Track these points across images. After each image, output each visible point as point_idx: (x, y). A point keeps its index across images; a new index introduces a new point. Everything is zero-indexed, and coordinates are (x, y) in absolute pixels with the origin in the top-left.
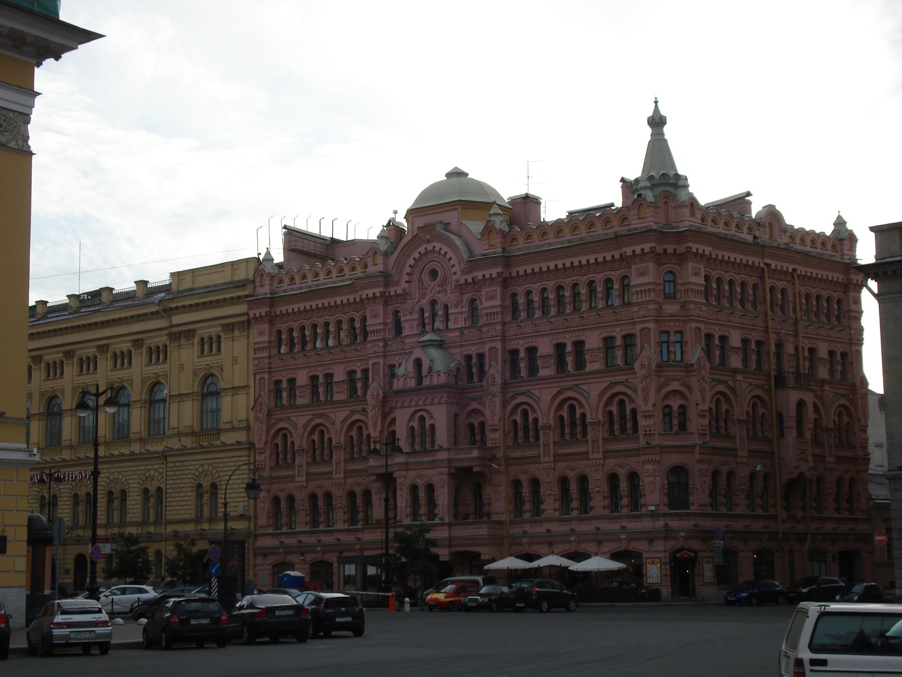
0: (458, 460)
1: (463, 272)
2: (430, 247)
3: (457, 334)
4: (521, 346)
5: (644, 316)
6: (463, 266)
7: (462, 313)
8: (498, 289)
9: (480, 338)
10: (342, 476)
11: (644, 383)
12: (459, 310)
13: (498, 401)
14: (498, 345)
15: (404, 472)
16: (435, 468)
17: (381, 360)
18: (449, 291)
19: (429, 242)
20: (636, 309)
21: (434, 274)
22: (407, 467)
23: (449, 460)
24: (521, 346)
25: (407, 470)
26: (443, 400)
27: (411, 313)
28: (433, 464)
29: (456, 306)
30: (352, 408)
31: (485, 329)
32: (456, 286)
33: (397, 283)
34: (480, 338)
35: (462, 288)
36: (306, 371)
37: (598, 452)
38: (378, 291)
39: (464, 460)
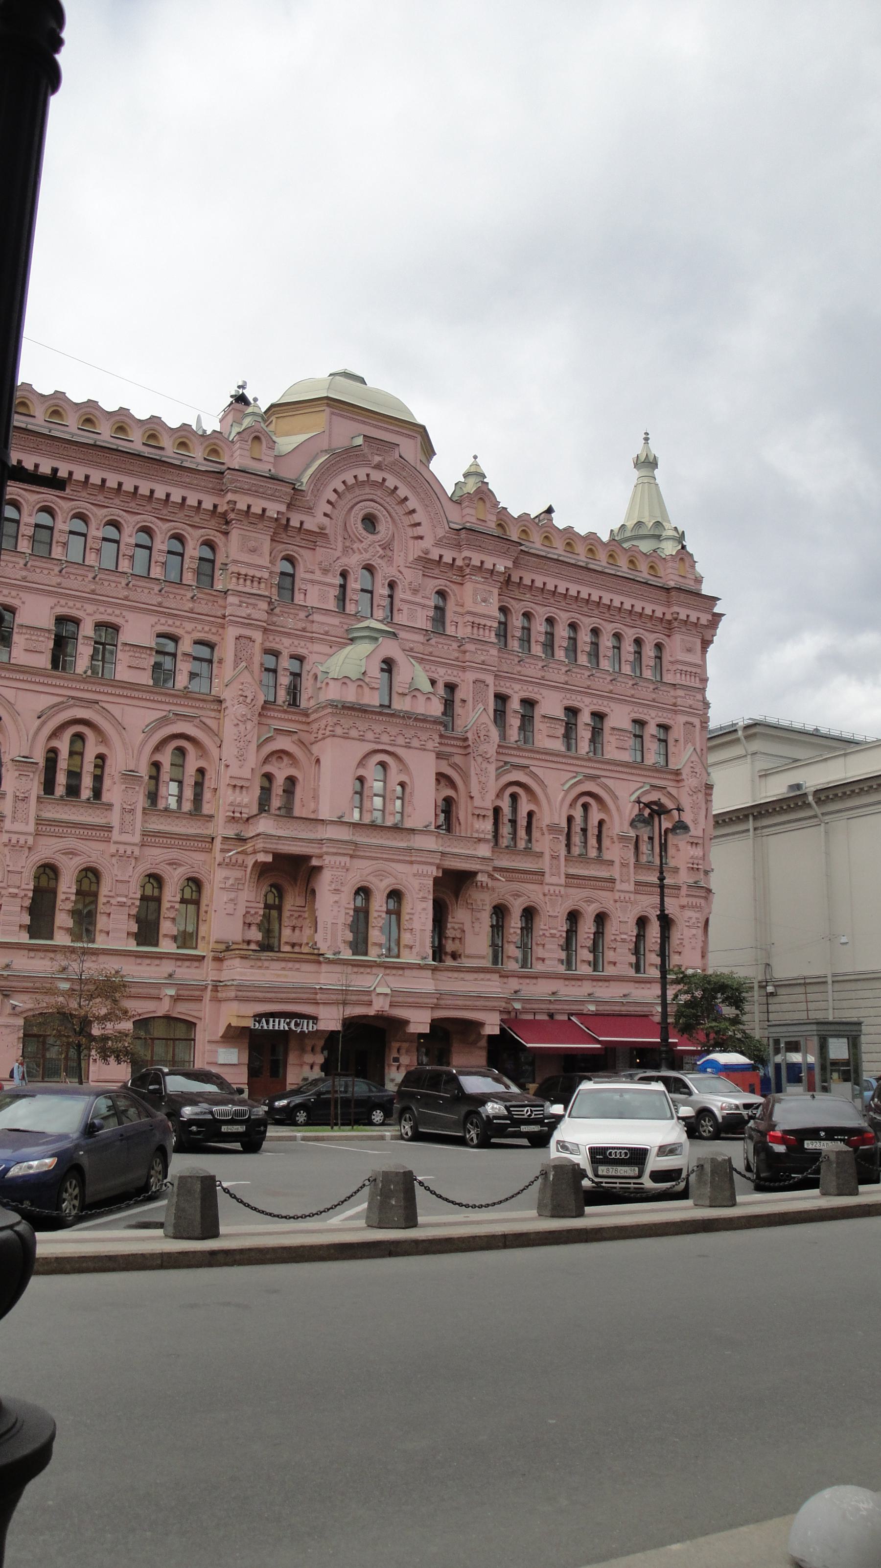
0: (454, 855)
1: (439, 543)
2: (376, 476)
3: (420, 638)
4: (517, 694)
5: (690, 707)
6: (441, 533)
7: (424, 606)
8: (496, 591)
9: (457, 659)
10: (137, 839)
11: (695, 797)
12: (418, 599)
13: (492, 768)
14: (490, 679)
15: (347, 859)
16: (411, 863)
17: (258, 636)
18: (399, 559)
19: (378, 467)
20: (680, 693)
21: (370, 521)
22: (354, 851)
23: (443, 854)
24: (517, 694)
25: (352, 856)
26: (430, 745)
27: (325, 571)
28: (409, 855)
29: (415, 591)
30: (168, 707)
31: (470, 647)
32: (419, 559)
33: (309, 510)
34: (457, 659)
35: (426, 564)
36: (52, 601)
37: (628, 881)
38: (274, 508)
39: (468, 857)
